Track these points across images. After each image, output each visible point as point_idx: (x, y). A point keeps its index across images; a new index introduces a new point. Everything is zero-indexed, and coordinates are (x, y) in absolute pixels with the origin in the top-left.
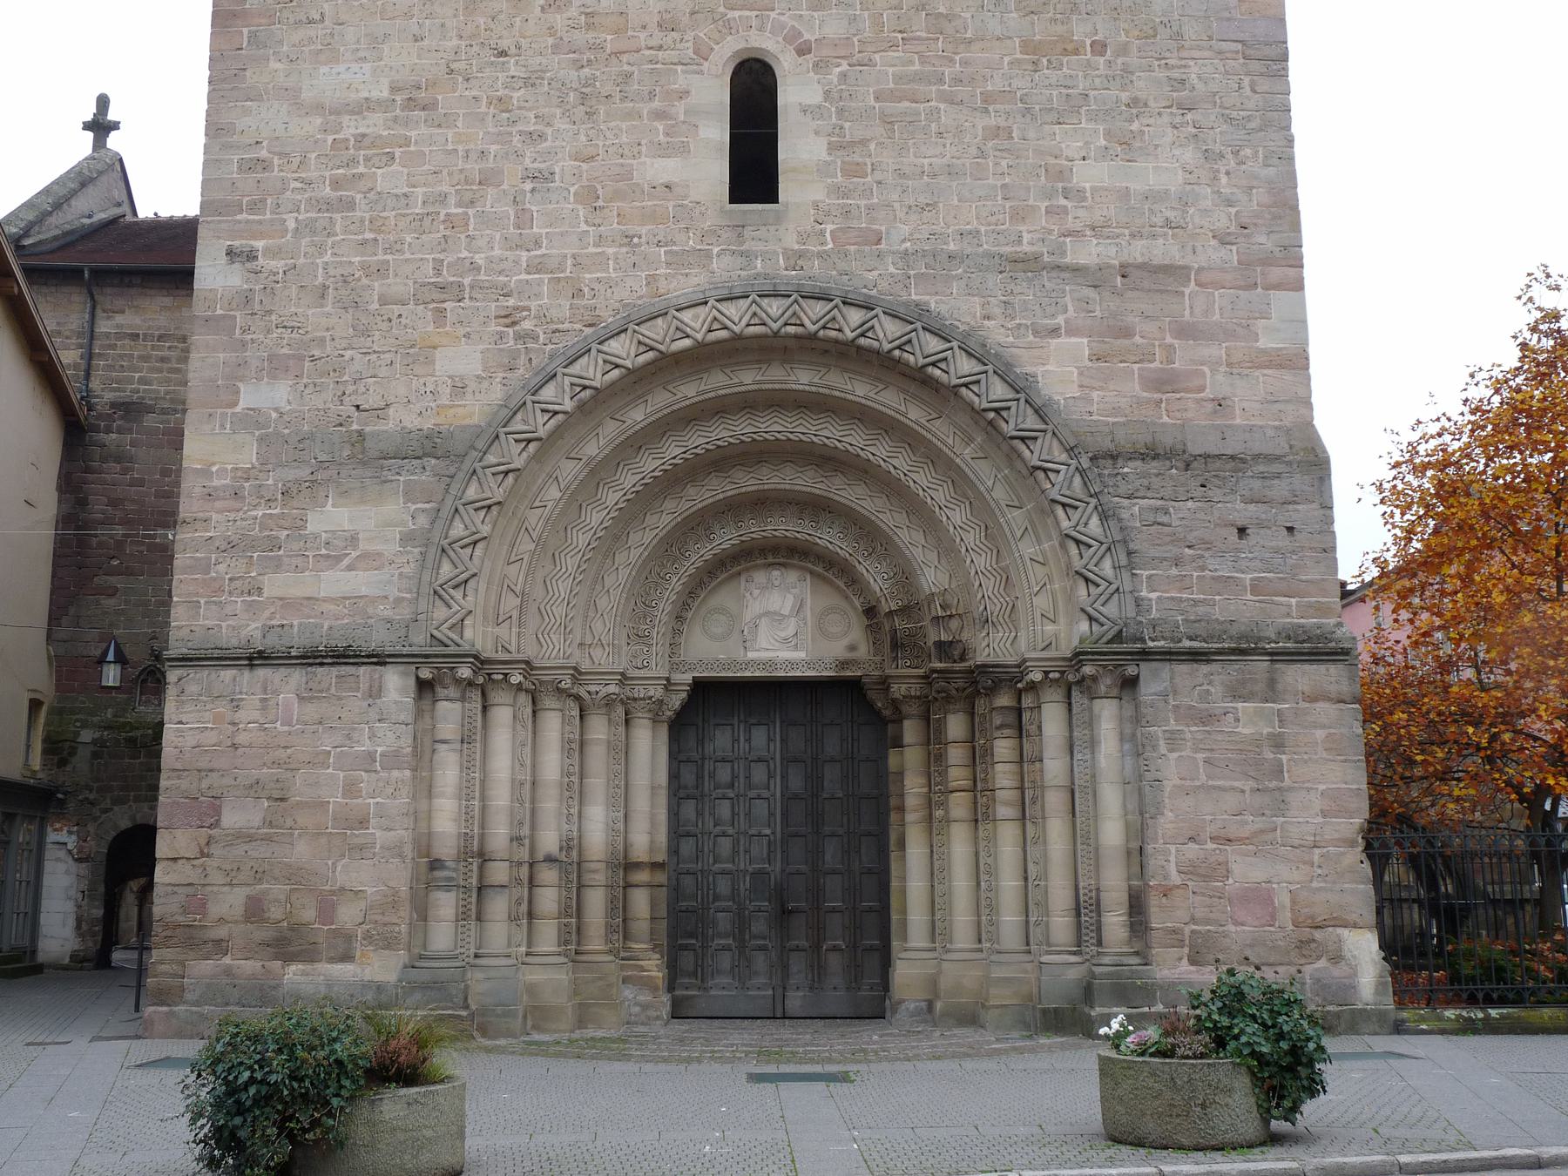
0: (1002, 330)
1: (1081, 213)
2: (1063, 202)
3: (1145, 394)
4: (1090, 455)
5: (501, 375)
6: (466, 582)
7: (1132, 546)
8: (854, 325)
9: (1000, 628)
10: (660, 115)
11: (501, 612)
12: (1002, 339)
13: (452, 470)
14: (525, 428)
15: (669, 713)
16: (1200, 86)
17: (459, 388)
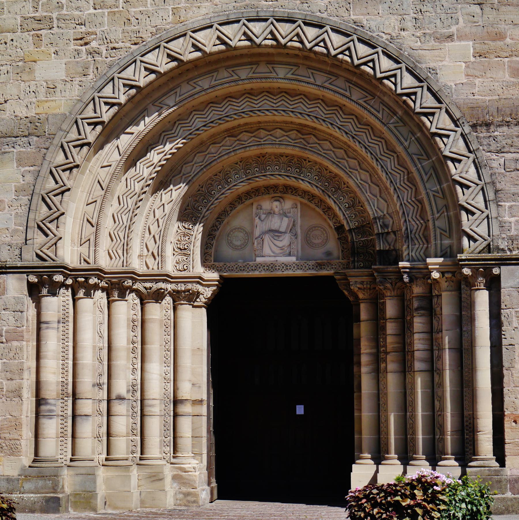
0: (413, 38)
3: (512, 79)
4: (471, 123)
5: (78, 79)
6: (57, 218)
7: (499, 186)
8: (310, 38)
9: (416, 242)
11: (83, 237)
12: (412, 45)
13: (47, 144)
14: (95, 115)
15: (204, 300)
17: (52, 88)
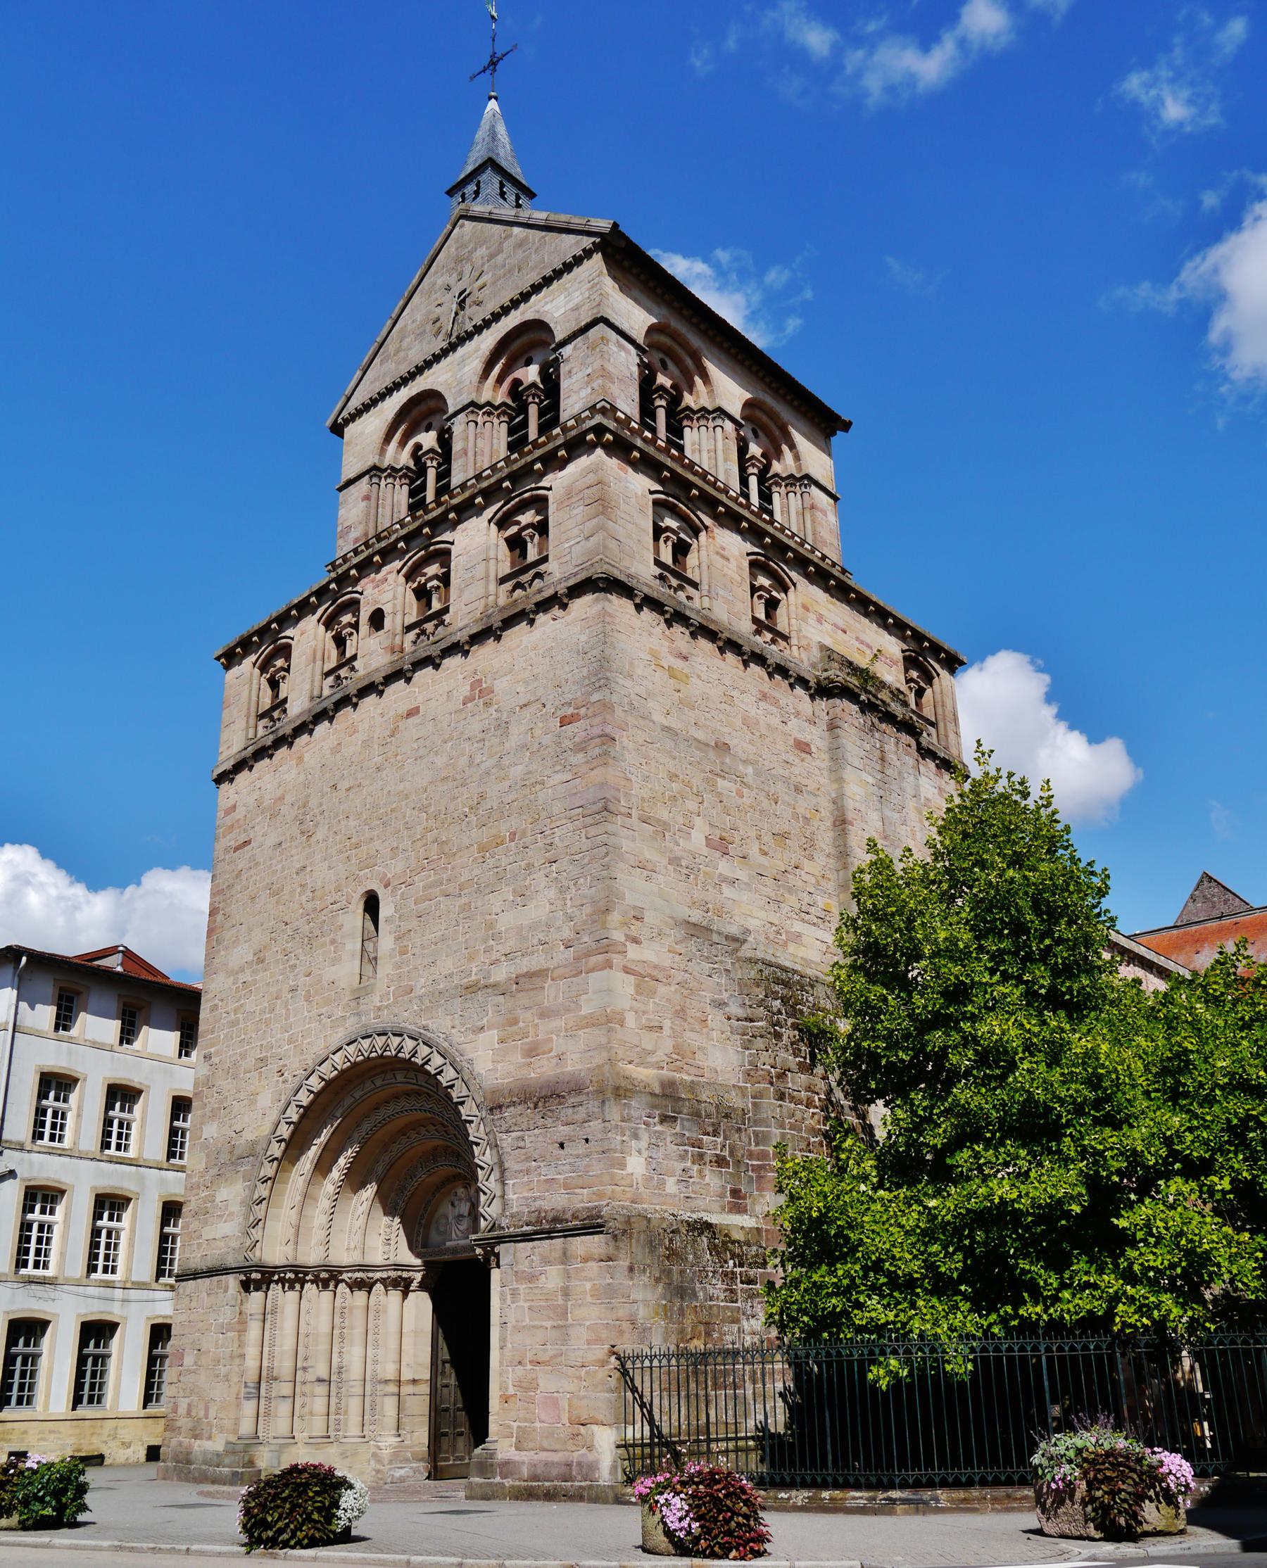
1: (500, 947)
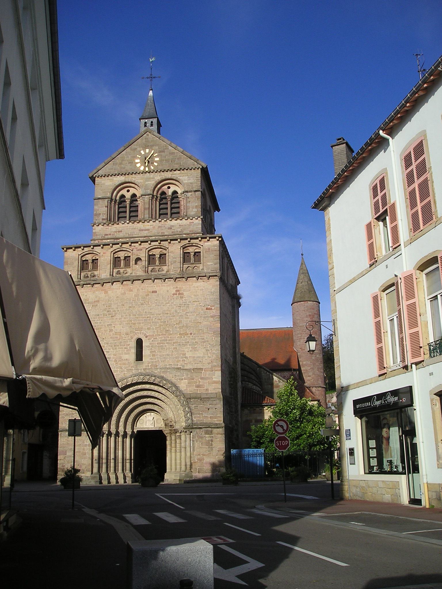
2: (185, 359)
10: (125, 348)
16: (206, 339)
